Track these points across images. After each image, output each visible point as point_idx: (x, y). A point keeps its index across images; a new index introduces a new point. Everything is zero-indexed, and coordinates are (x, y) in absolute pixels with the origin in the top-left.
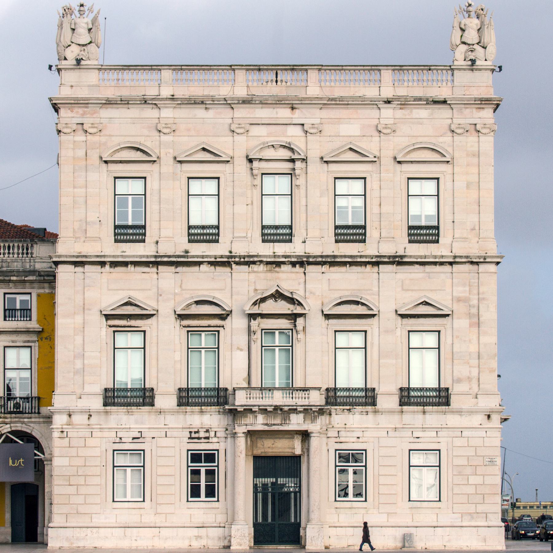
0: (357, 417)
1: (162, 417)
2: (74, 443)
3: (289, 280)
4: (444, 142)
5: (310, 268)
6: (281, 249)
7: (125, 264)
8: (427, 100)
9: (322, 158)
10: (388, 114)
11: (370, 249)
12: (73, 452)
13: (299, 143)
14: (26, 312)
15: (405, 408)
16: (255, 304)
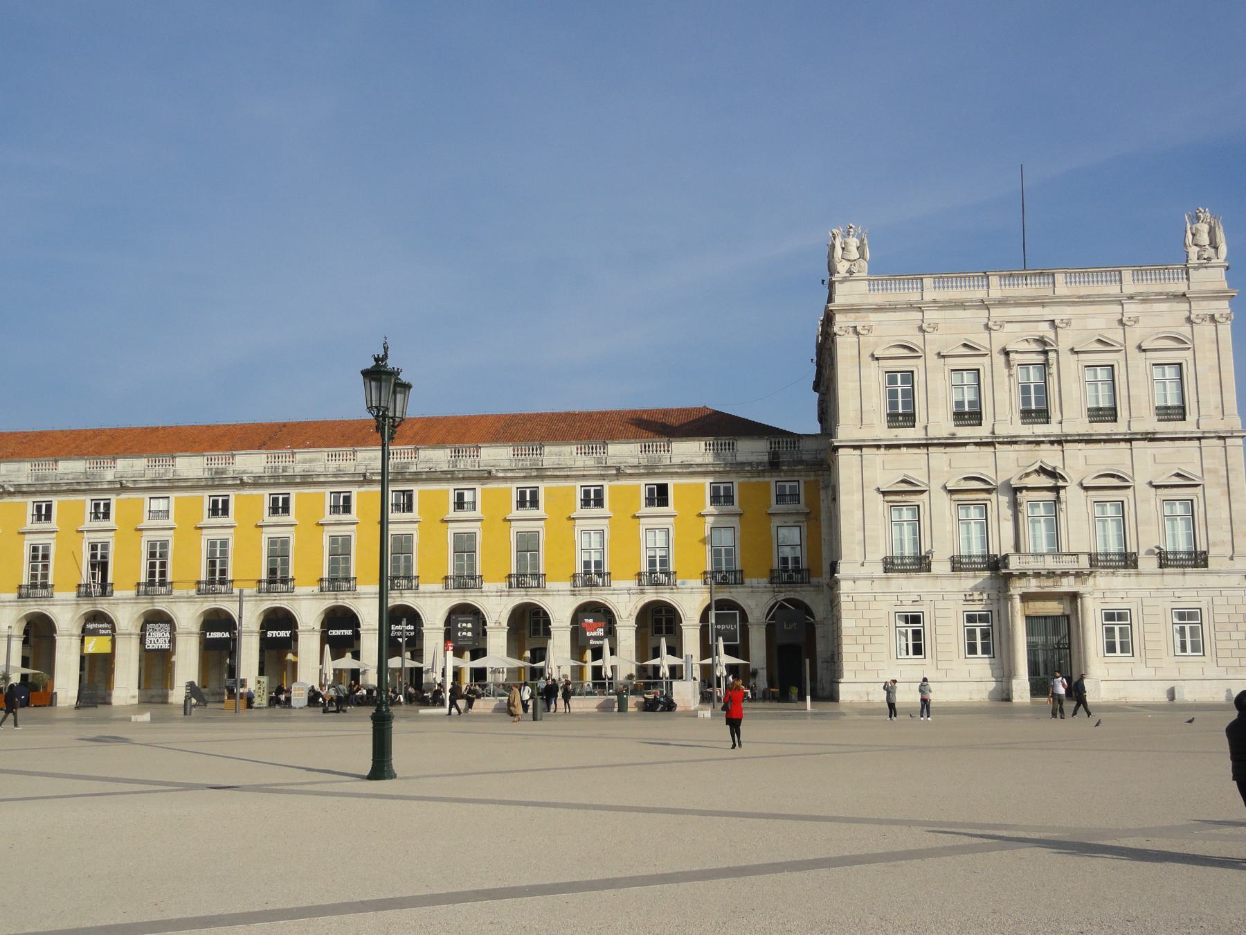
0: (1120, 579)
1: (939, 581)
2: (860, 606)
3: (1050, 457)
4: (1185, 330)
5: (1067, 446)
6: (1040, 429)
7: (898, 446)
8: (1167, 294)
9: (1072, 350)
10: (1132, 309)
11: (1120, 428)
12: (859, 614)
13: (1049, 334)
14: (795, 497)
15: (1166, 570)
16: (1021, 478)
